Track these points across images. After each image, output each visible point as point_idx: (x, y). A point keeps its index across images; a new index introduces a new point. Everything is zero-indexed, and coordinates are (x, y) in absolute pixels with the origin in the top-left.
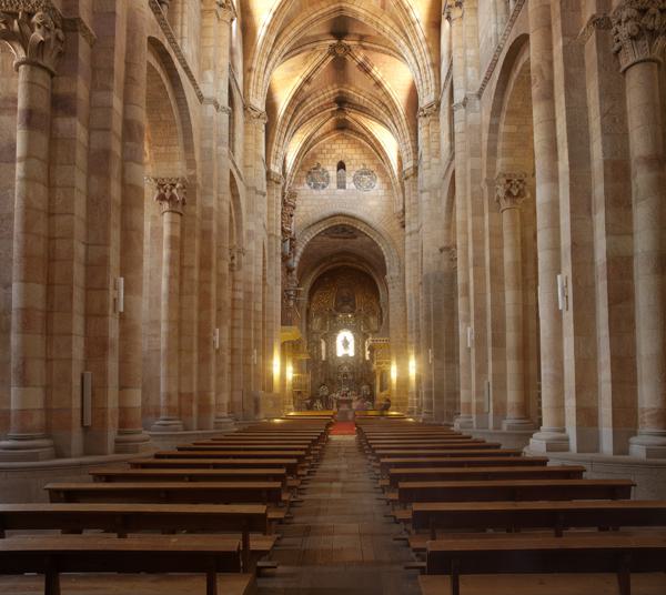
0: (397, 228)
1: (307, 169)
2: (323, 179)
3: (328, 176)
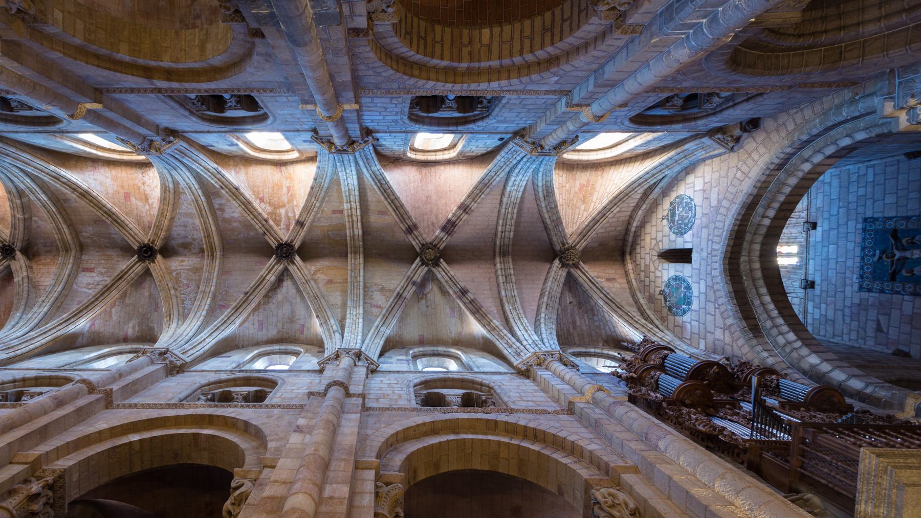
0: (760, 136)
1: (665, 310)
2: (678, 288)
3: (676, 279)
